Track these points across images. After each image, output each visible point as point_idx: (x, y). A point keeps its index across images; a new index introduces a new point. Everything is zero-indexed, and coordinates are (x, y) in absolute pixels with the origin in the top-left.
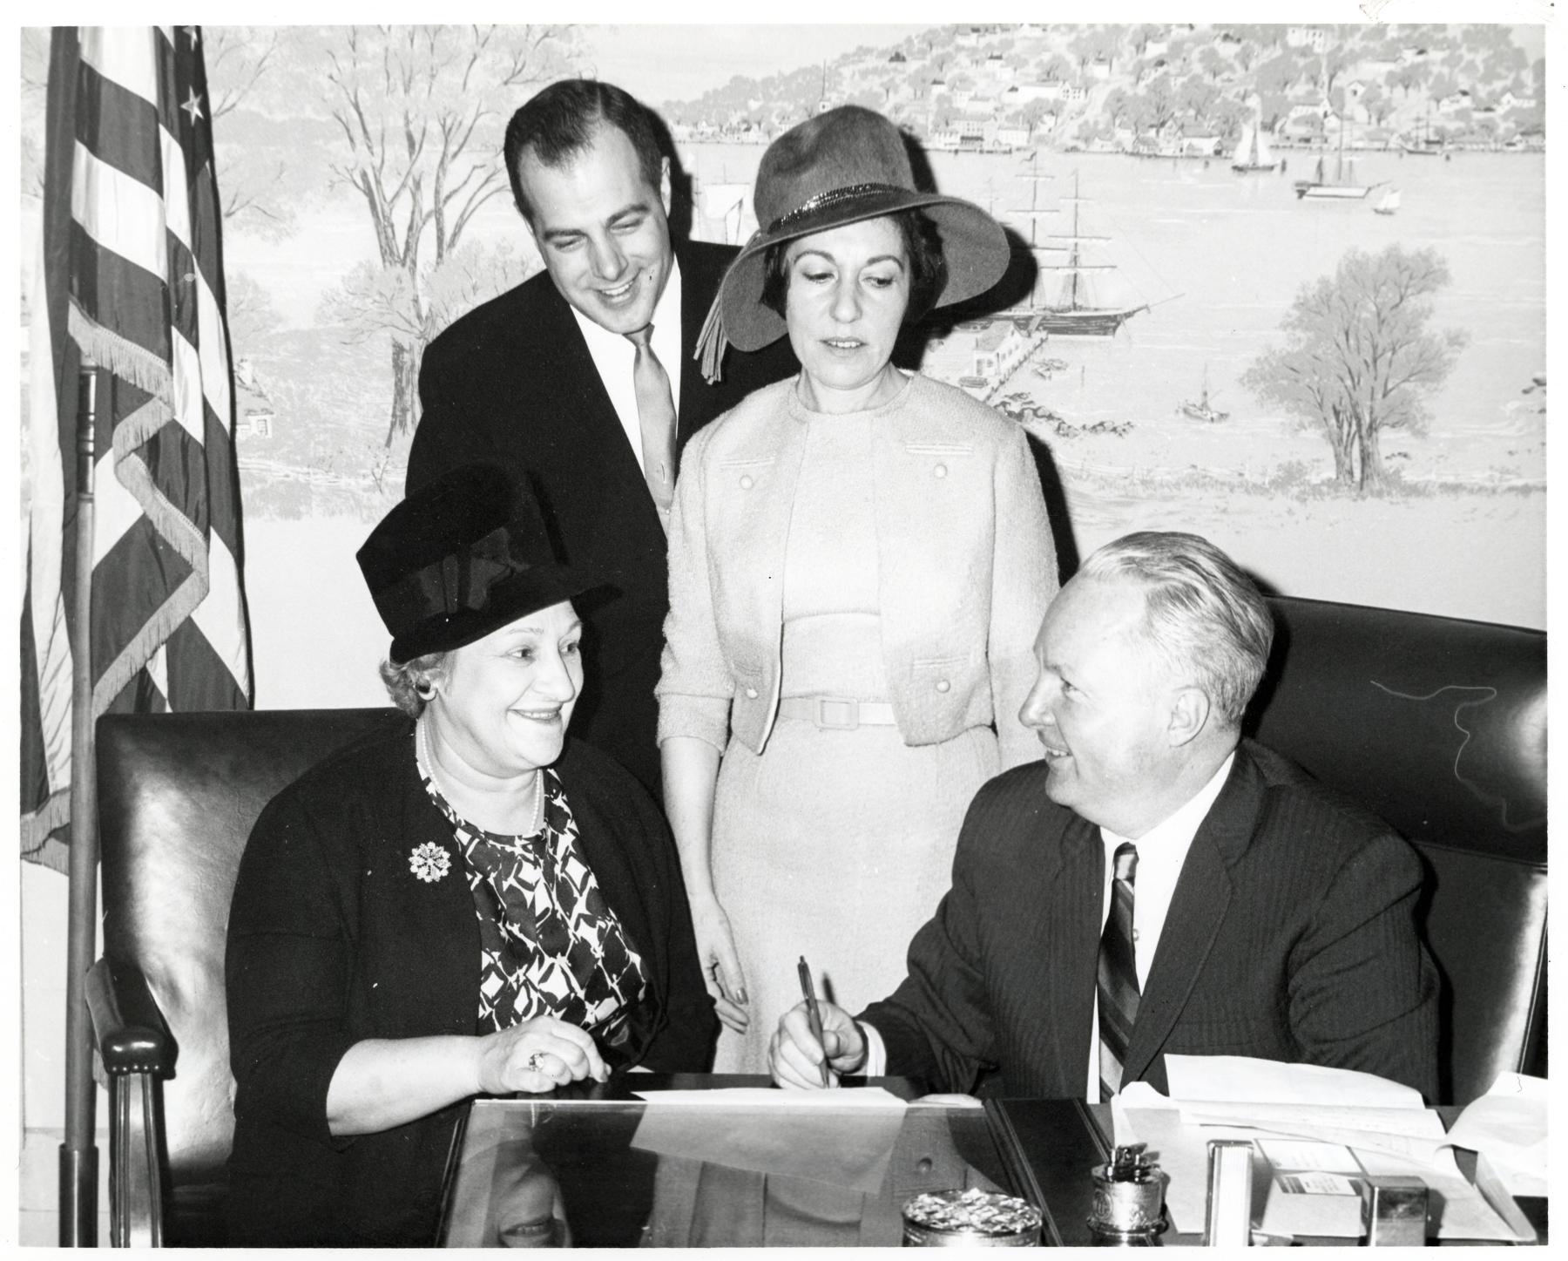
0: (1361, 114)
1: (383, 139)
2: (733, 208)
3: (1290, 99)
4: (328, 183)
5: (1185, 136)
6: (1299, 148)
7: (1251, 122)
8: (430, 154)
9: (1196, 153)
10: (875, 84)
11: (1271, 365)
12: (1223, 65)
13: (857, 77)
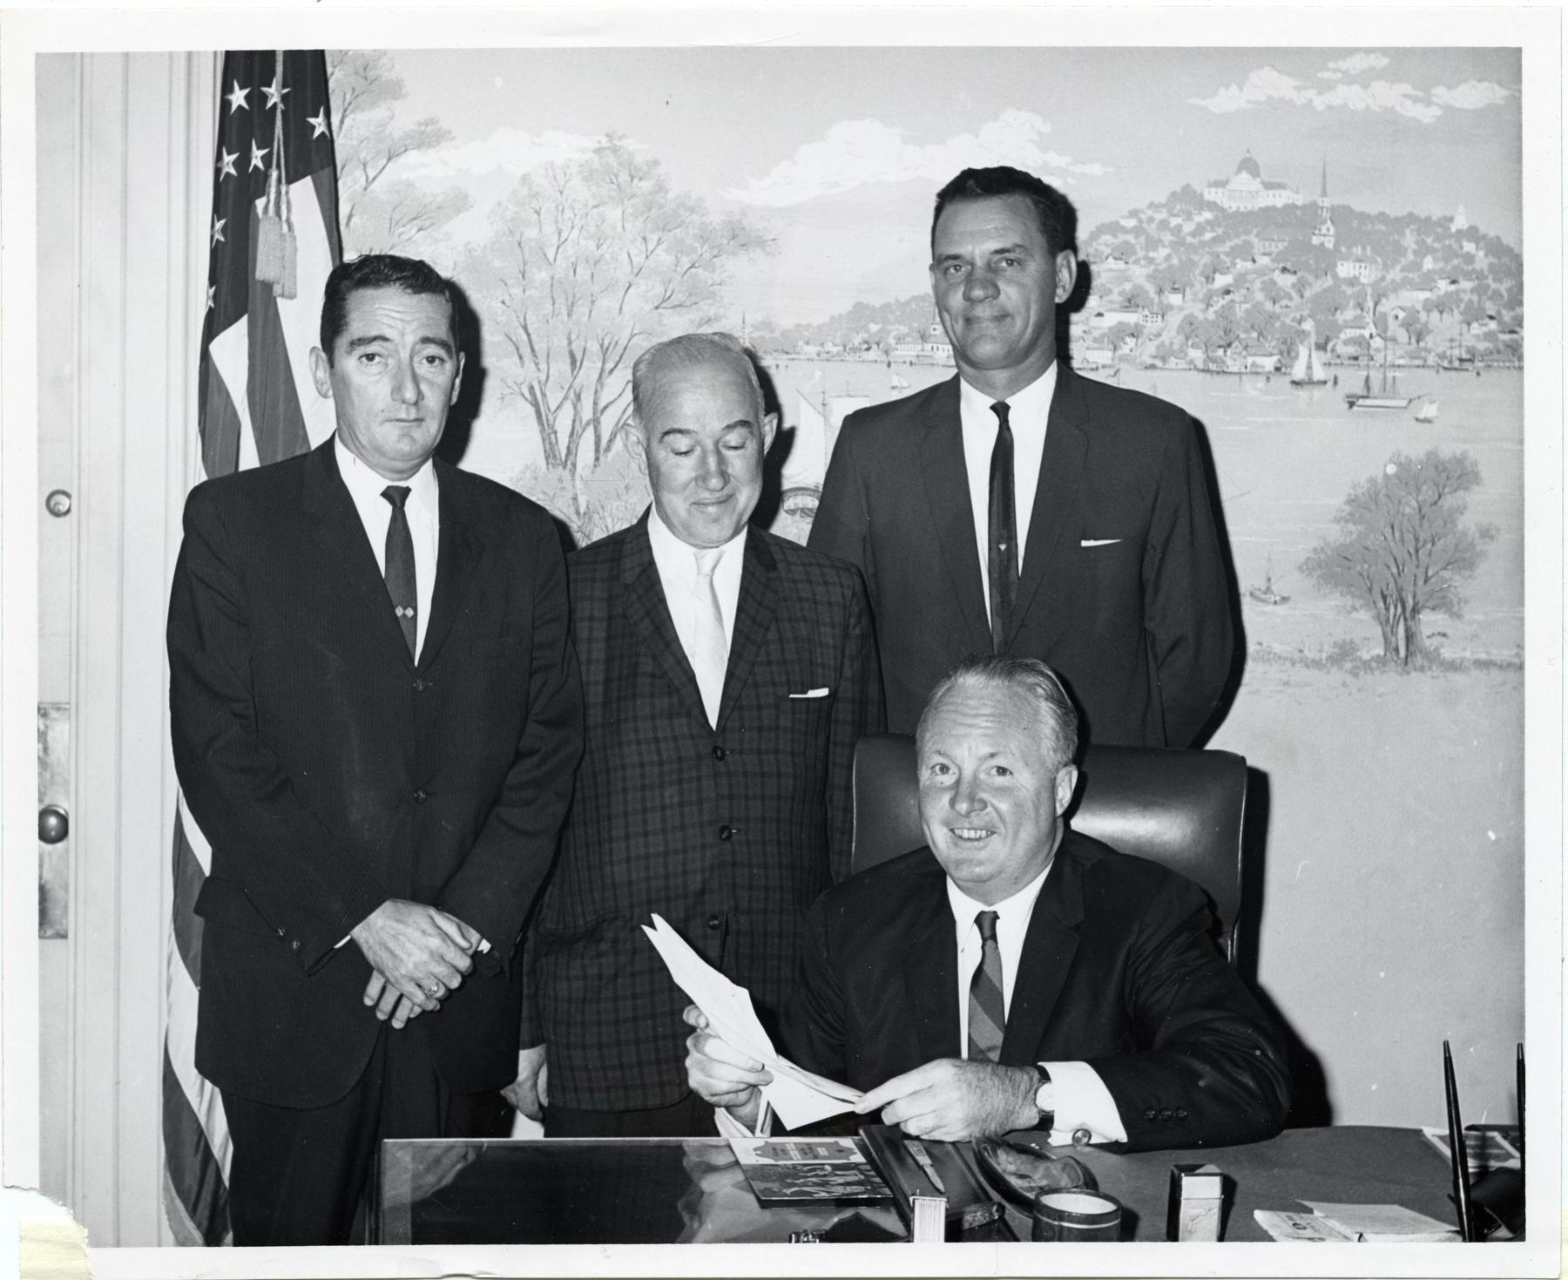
0: (1402, 336)
1: (548, 357)
3: (1340, 322)
4: (500, 396)
5: (1250, 355)
6: (1349, 365)
7: (1306, 343)
8: (590, 370)
9: (1259, 370)
11: (1326, 554)
12: (1282, 293)
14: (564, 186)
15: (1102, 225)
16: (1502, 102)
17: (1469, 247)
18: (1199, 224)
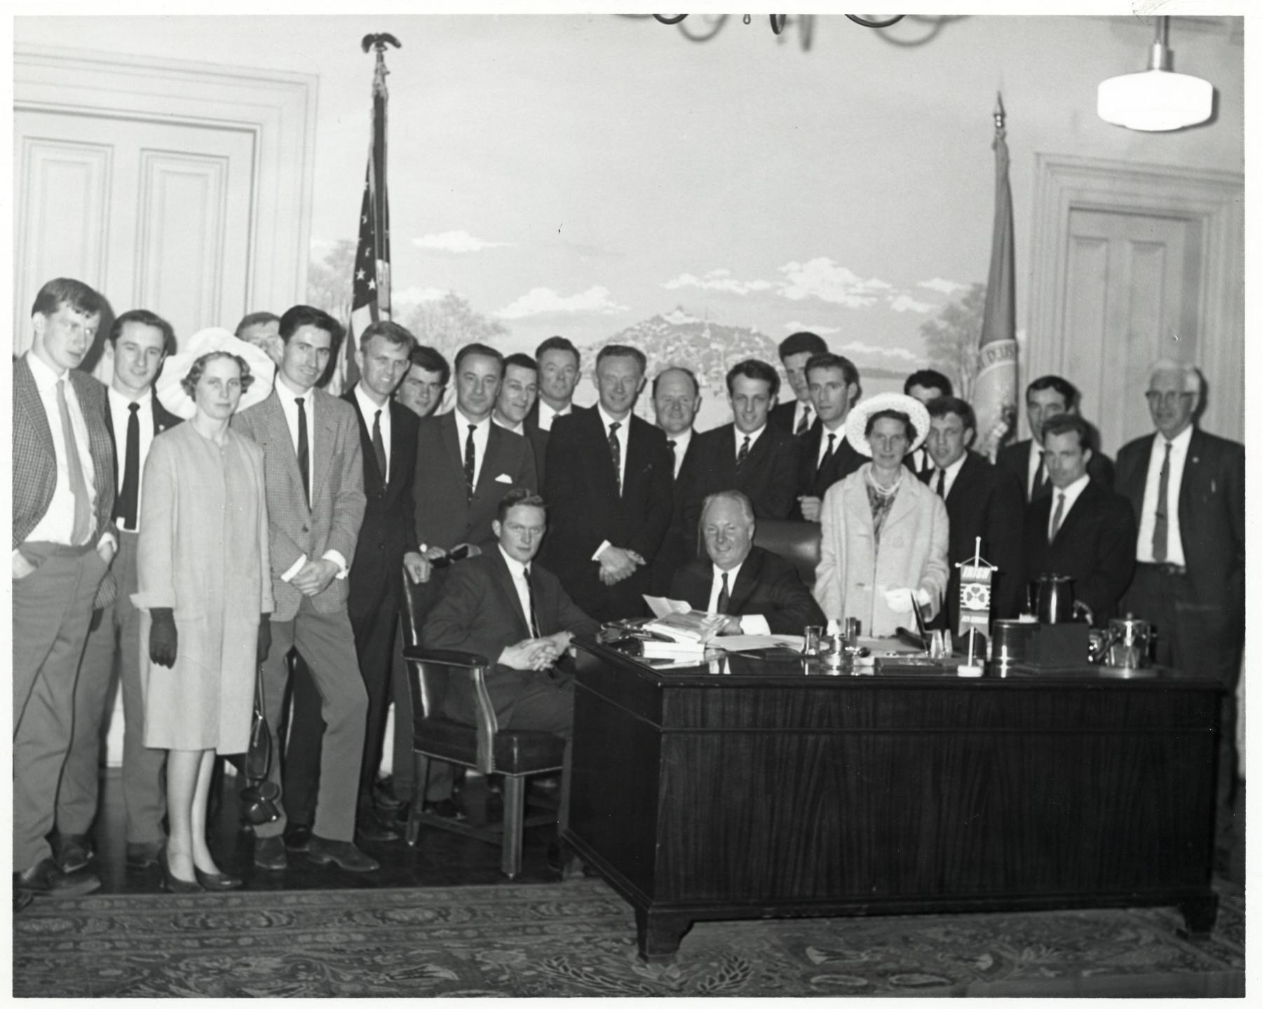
17: (757, 339)
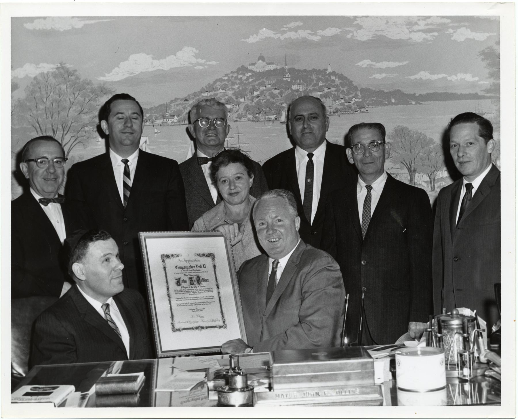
2: (144, 143)
7: (284, 111)
9: (270, 120)
10: (180, 107)
13: (175, 106)
14: (47, 80)
15: (217, 79)
16: (340, 33)
17: (333, 78)
18: (247, 77)
